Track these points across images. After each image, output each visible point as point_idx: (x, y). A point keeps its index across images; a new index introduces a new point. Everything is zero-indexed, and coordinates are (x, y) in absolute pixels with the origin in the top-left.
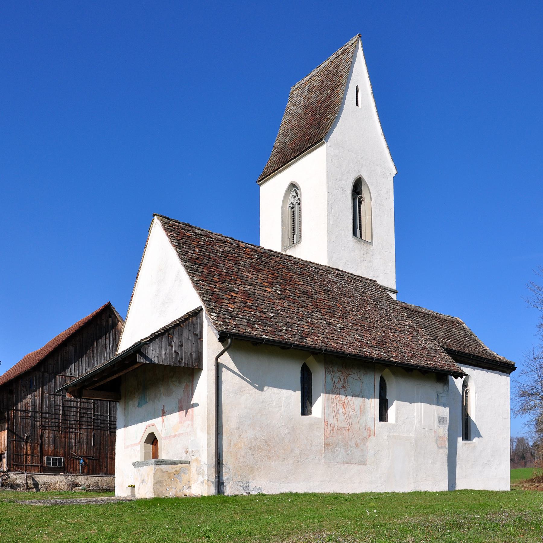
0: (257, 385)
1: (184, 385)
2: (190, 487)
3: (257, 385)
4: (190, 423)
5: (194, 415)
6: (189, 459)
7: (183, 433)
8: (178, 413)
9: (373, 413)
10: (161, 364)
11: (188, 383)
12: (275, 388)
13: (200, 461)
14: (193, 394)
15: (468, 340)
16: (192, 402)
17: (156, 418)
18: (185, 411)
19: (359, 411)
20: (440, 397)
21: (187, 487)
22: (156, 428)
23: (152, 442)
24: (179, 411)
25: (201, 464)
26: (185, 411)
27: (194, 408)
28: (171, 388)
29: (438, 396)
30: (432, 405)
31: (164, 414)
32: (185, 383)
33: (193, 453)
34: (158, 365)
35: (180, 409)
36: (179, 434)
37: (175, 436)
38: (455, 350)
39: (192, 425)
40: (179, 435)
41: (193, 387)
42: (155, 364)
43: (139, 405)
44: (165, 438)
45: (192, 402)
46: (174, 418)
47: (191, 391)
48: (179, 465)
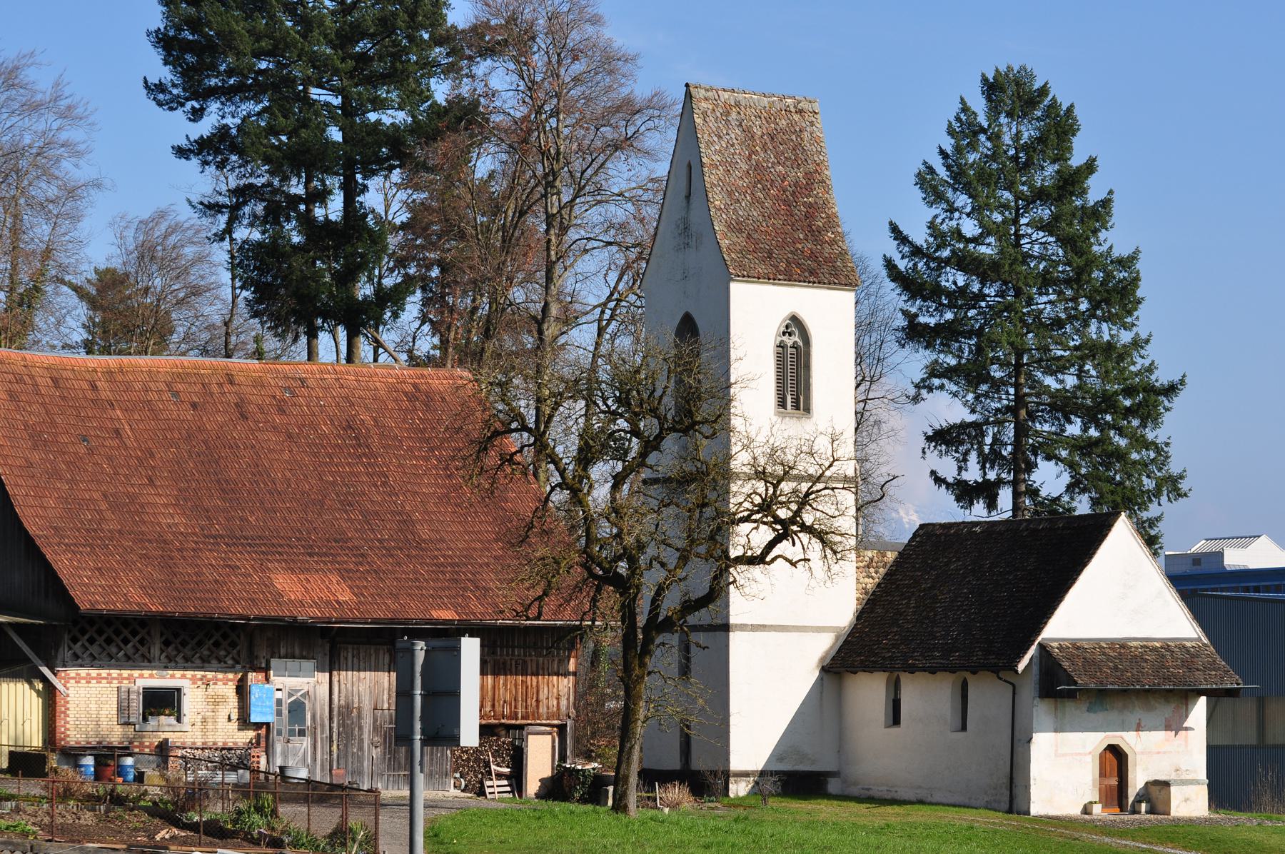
1: (1173, 705)
14: (1187, 717)
18: (1174, 732)
26: (1174, 732)
35: (1168, 728)
37: (1159, 753)
39: (1186, 746)
40: (1165, 753)
44: (1142, 753)
46: (1161, 735)
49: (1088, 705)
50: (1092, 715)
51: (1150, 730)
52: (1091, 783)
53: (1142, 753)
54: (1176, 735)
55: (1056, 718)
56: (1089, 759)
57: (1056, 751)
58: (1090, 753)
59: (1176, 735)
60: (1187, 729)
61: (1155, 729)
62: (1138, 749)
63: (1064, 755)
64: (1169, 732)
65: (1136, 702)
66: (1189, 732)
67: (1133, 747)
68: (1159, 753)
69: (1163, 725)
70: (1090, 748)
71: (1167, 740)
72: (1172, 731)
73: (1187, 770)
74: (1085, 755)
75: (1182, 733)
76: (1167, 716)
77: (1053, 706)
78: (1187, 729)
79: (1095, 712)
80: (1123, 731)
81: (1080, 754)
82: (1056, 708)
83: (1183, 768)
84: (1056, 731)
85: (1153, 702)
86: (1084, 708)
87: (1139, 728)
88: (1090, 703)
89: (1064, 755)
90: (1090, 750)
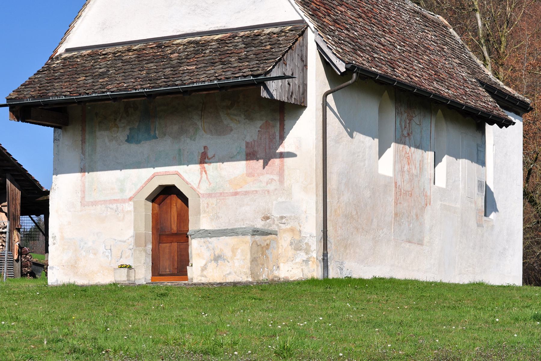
0: (349, 130)
1: (259, 123)
2: (278, 267)
3: (349, 130)
4: (276, 178)
5: (285, 167)
6: (274, 228)
7: (256, 191)
8: (244, 163)
9: (429, 172)
10: (279, 100)
11: (270, 122)
12: (360, 134)
13: (300, 231)
14: (282, 138)
15: (466, 57)
16: (280, 150)
17: (183, 165)
18: (261, 162)
19: (419, 169)
20: (479, 152)
21: (276, 267)
22: (183, 179)
23: (152, 198)
24: (247, 160)
25: (303, 235)
26: (261, 162)
27: (286, 160)
28: (225, 123)
29: (478, 150)
30: (473, 163)
31: (206, 160)
32: (262, 120)
33: (284, 221)
34: (276, 100)
35: (250, 156)
36: (246, 191)
37: (236, 194)
38: (484, 82)
39: (281, 181)
40: (246, 193)
41: (284, 129)
42: (274, 99)
43: (129, 140)
44: (210, 195)
45: (280, 150)
47: (277, 134)
48: (269, 236)
49: (127, 132)
50: (134, 147)
51: (222, 160)
52: (132, 240)
53: (210, 195)
54: (265, 164)
55: (83, 153)
56: (129, 207)
57: (83, 198)
58: (131, 199)
59: (265, 164)
60: (282, 155)
61: (231, 158)
62: (203, 189)
63: (95, 203)
64: (253, 163)
65: (199, 123)
66: (287, 160)
67: (195, 186)
68: (236, 194)
69: (244, 156)
70: (129, 194)
71: (249, 175)
72: (257, 159)
73: (282, 218)
74: (124, 201)
75: (276, 162)
76: (248, 139)
77: (80, 138)
78: (282, 155)
79: (138, 142)
80: (180, 164)
81: (116, 201)
82: (83, 141)
83: (276, 214)
84: (83, 170)
85: (226, 121)
86: (122, 135)
87: (204, 159)
88: (130, 129)
89: (95, 203)
90: (131, 194)
